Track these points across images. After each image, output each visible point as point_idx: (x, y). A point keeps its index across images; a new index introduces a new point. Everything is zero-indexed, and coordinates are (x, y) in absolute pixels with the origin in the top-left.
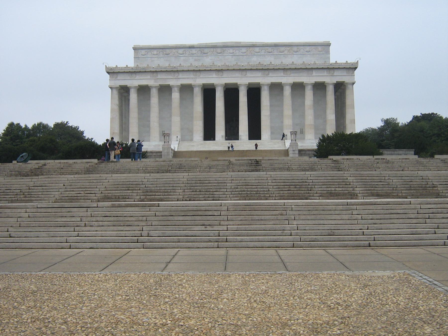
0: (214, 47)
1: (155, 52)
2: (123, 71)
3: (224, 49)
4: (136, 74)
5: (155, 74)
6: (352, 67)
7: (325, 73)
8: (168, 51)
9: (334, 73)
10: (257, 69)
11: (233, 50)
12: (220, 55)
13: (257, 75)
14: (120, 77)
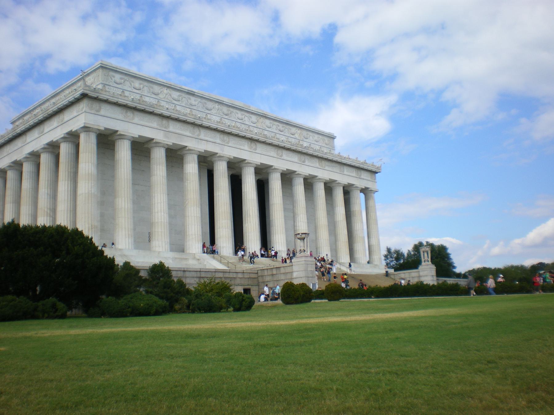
2: (115, 100)
3: (231, 109)
4: (133, 114)
5: (165, 122)
6: (377, 171)
7: (353, 173)
11: (242, 115)
12: (226, 117)
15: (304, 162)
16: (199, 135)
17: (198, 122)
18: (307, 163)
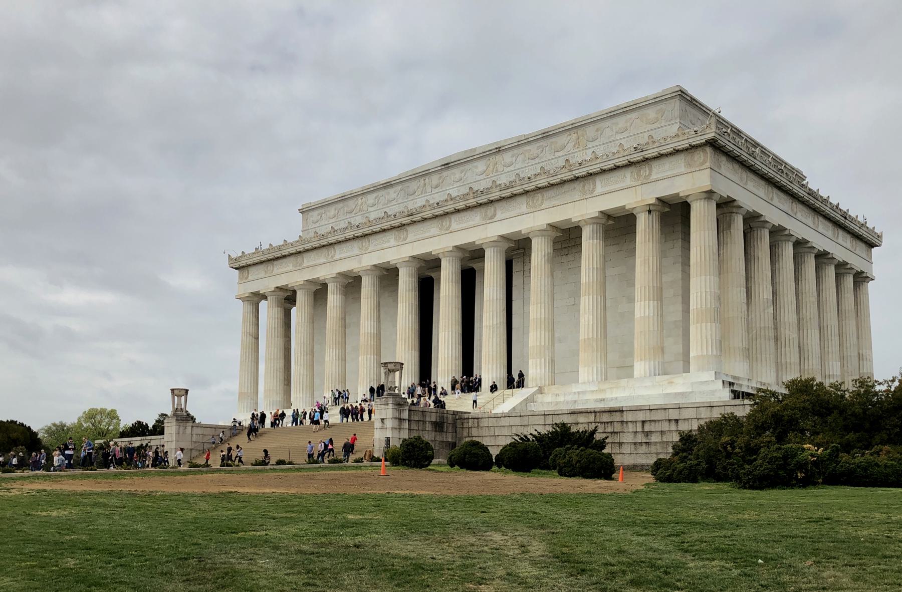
0: (424, 174)
1: (332, 211)
3: (445, 174)
5: (299, 258)
7: (628, 177)
8: (351, 204)
9: (650, 174)
10: (468, 208)
13: (471, 223)
14: (254, 273)
15: (495, 215)
16: (332, 257)
17: (324, 242)
18: (499, 215)
